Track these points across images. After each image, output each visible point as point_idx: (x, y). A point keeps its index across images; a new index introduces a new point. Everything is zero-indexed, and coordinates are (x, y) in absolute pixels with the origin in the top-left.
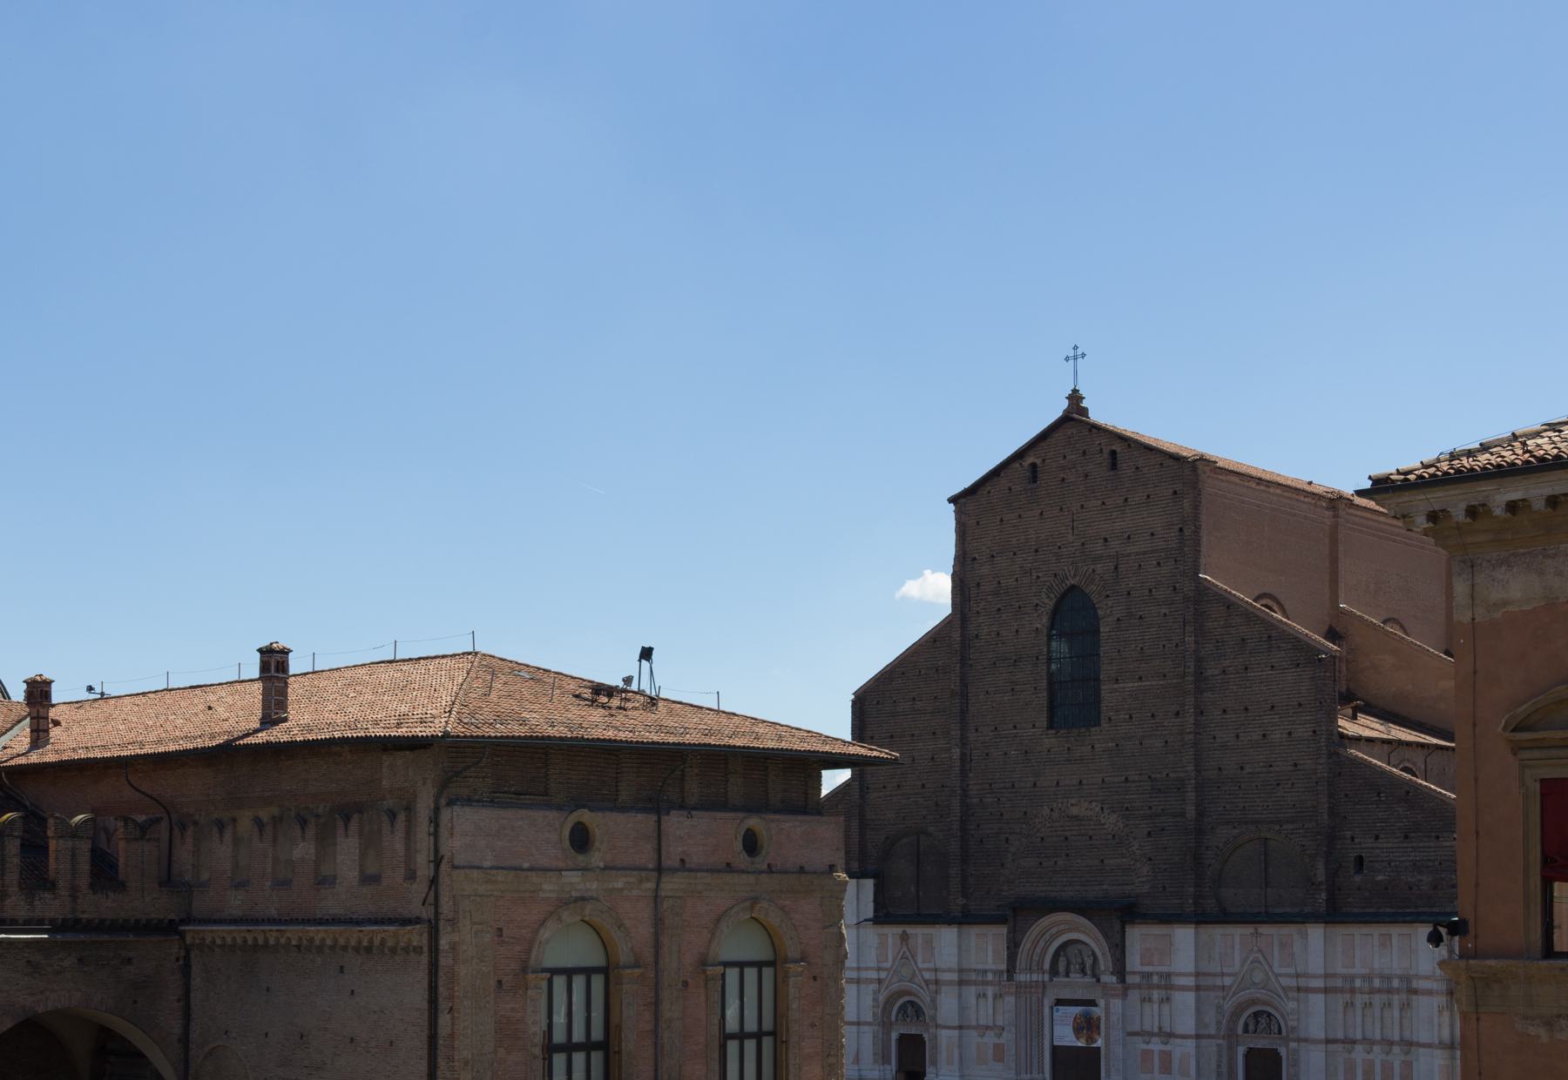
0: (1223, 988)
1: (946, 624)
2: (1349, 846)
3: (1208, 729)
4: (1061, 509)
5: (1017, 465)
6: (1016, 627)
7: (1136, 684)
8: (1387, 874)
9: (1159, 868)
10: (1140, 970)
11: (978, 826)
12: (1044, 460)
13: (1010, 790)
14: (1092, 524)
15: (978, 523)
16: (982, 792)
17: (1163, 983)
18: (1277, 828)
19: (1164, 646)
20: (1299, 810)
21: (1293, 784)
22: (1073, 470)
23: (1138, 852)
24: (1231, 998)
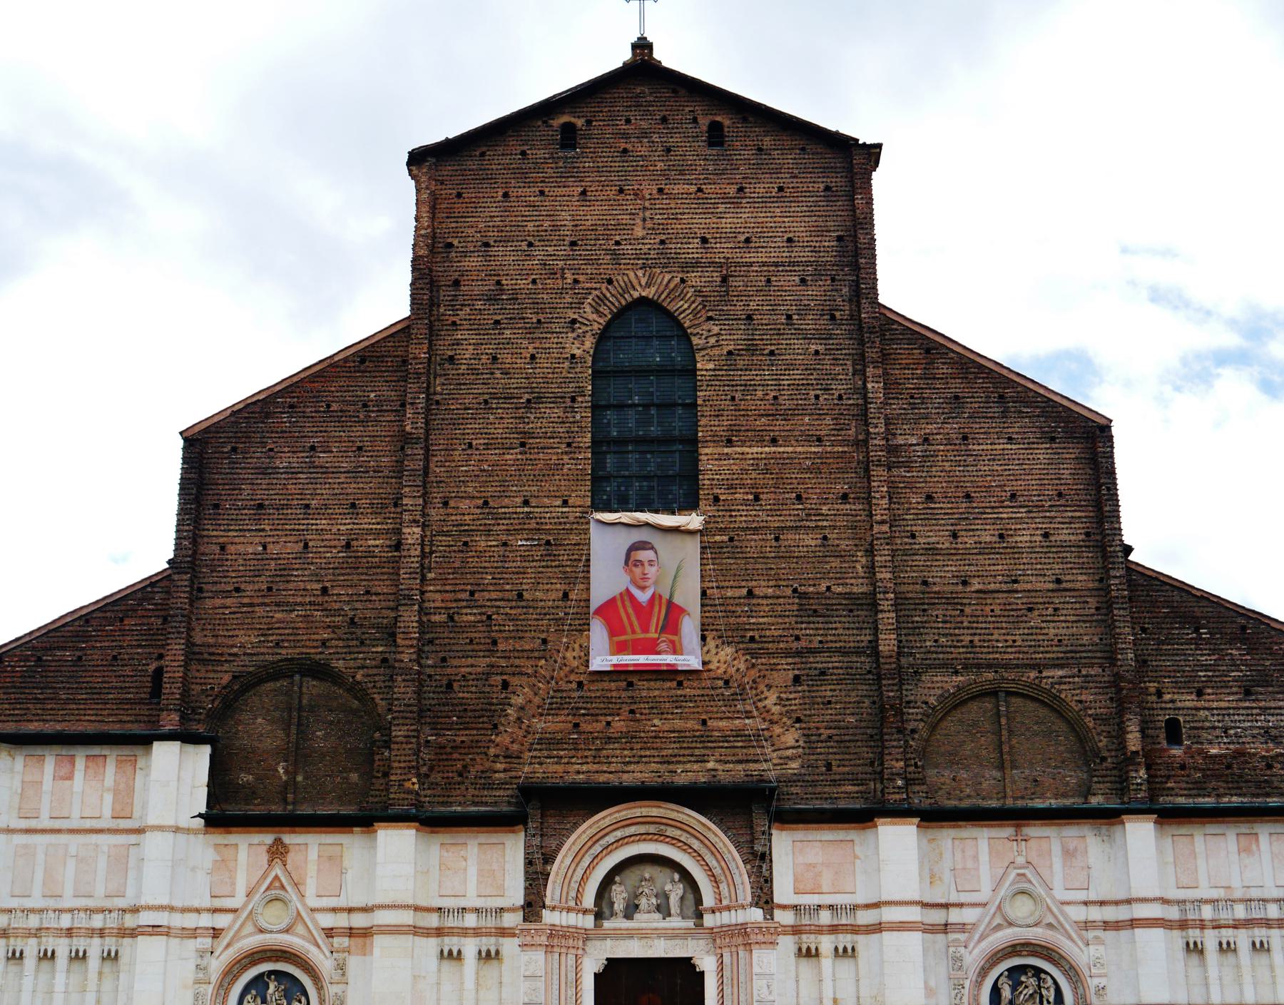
0: (962, 927)
1: (399, 334)
2: (1155, 705)
3: (905, 523)
4: (621, 191)
5: (540, 123)
6: (531, 350)
7: (767, 449)
8: (1222, 745)
9: (820, 735)
10: (796, 902)
11: (444, 660)
12: (589, 122)
13: (514, 604)
14: (679, 216)
15: (459, 195)
16: (454, 605)
17: (844, 922)
18: (1033, 674)
19: (817, 397)
20: (1069, 648)
21: (1056, 610)
22: (646, 140)
23: (776, 709)
24: (979, 941)
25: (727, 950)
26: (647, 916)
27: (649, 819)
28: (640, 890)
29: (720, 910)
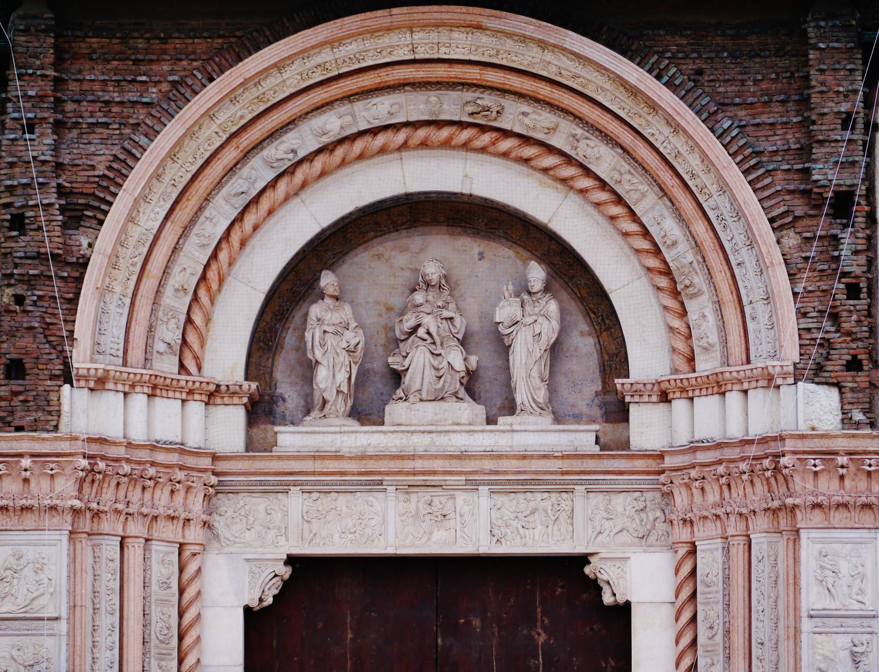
25: (711, 528)
26: (429, 410)
27: (440, 72)
28: (409, 321)
29: (689, 393)
